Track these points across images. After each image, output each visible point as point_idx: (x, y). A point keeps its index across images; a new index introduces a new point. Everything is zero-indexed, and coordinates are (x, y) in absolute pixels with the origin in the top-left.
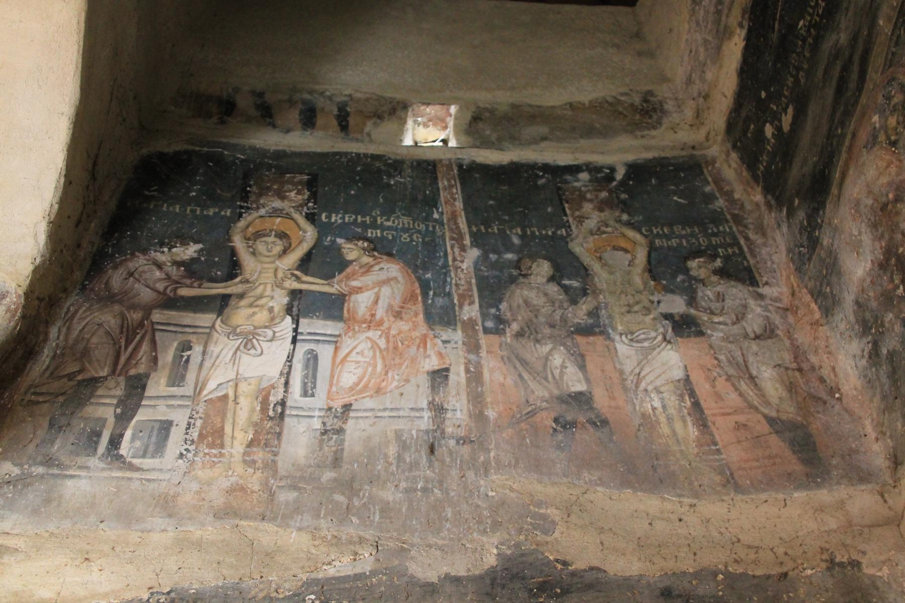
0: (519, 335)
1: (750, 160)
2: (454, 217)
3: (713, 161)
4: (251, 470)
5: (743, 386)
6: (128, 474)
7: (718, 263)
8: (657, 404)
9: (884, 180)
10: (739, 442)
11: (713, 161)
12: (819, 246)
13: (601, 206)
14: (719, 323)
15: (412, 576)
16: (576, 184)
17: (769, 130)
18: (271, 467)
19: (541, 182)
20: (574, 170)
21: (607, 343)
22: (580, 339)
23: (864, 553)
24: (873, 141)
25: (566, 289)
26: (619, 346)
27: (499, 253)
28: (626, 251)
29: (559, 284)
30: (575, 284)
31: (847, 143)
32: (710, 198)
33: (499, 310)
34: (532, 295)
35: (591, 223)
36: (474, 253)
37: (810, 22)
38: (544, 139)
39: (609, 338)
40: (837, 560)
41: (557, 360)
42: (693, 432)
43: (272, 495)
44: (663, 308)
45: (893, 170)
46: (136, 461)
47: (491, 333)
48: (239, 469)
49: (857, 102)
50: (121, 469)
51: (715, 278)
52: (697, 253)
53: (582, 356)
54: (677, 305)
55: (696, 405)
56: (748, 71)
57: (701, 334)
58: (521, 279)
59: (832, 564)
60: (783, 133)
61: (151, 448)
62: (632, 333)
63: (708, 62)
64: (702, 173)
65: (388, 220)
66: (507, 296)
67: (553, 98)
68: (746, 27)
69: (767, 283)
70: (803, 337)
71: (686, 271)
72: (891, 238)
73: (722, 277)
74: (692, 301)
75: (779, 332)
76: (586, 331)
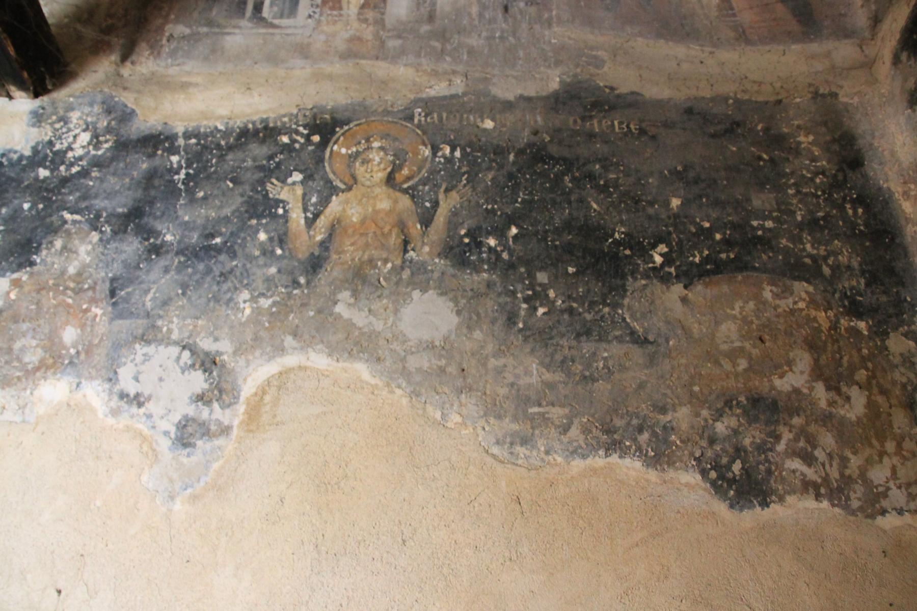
4: (364, 26)
6: (271, 31)
10: (751, 8)
15: (494, 97)
18: (380, 23)
23: (841, 87)
40: (821, 91)
43: (383, 43)
46: (276, 22)
48: (356, 25)
50: (264, 27)
59: (816, 95)
61: (286, 11)
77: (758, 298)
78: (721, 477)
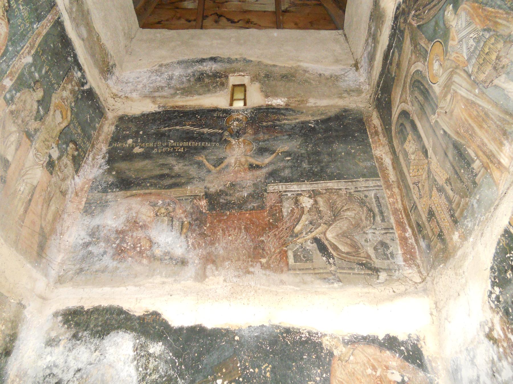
0: (12, 112)
1: (116, 138)
2: (39, 35)
3: (107, 119)
5: (45, 205)
7: (76, 153)
8: (22, 189)
9: (144, 218)
10: (29, 228)
11: (107, 119)
12: (105, 194)
13: (72, 92)
14: (58, 175)
16: (75, 73)
17: (130, 141)
19: (69, 59)
20: (80, 69)
21: (29, 147)
22: (24, 136)
24: (154, 205)
25: (38, 112)
26: (31, 152)
27: (35, 70)
28: (62, 117)
29: (38, 107)
30: (42, 112)
31: (147, 191)
32: (95, 129)
33: (16, 94)
34: (29, 101)
35: (65, 94)
36: (29, 59)
37: (174, 146)
38: (83, 40)
39: (31, 146)
40: (22, 302)
41: (13, 138)
42: (21, 211)
44: (52, 151)
45: (149, 219)
47: (5, 100)
49: (160, 188)
51: (71, 157)
52: (75, 143)
53: (20, 145)
54: (55, 154)
55: (30, 200)
56: (146, 119)
57: (51, 173)
58: (31, 90)
60: (132, 150)
62: (38, 152)
63: (139, 92)
64: (101, 119)
65: (23, 6)
66: (23, 91)
67: (98, 25)
68: (160, 110)
69: (79, 176)
70: (70, 207)
71: (68, 146)
72: (128, 231)
73: (73, 159)
74: (59, 158)
75: (67, 196)
76: (29, 136)
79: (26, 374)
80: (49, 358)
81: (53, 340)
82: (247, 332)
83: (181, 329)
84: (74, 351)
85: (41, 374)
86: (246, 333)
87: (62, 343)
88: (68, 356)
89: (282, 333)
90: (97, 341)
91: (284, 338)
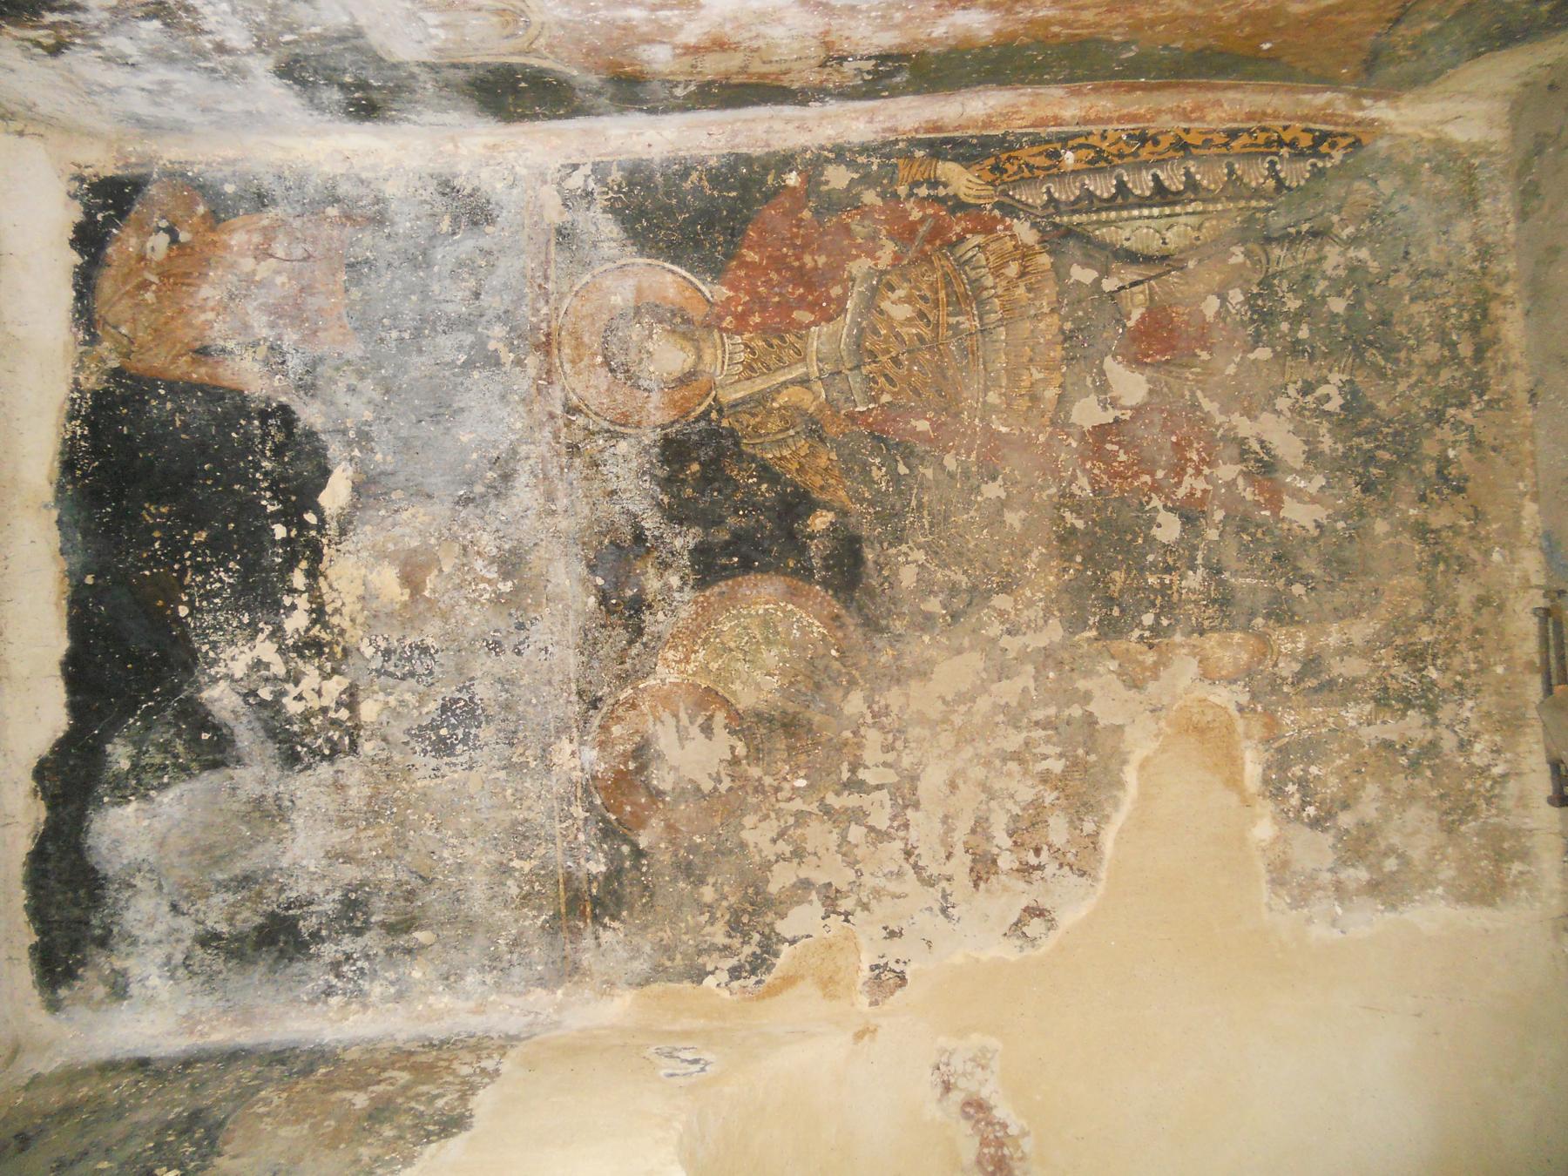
77: (260, 1116)
78: (438, 1134)
79: (187, 1017)
80: (154, 981)
81: (114, 985)
82: (74, 559)
83: (74, 708)
84: (136, 932)
85: (187, 984)
86: (77, 560)
87: (118, 965)
88: (146, 943)
89: (74, 481)
90: (111, 891)
91: (84, 476)
